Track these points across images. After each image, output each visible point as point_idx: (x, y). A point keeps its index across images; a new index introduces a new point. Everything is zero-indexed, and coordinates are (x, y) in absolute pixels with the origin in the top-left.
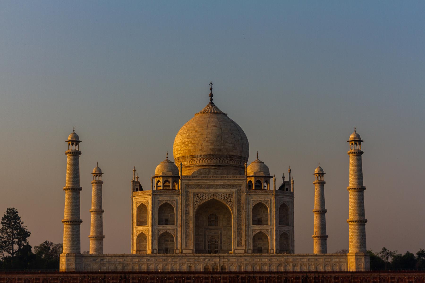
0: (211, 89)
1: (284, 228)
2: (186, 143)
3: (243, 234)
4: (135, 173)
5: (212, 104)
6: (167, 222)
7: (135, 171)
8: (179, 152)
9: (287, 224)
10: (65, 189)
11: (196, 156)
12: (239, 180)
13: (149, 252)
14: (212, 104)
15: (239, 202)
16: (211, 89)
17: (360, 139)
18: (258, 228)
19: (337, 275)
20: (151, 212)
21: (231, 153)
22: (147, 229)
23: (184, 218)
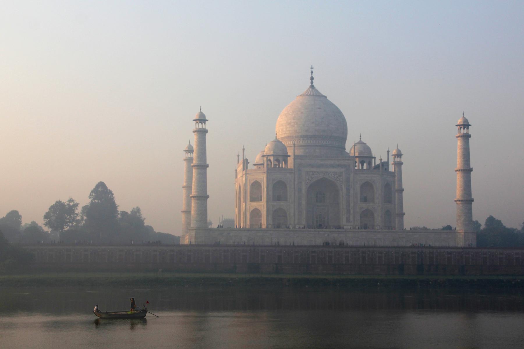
2: (292, 124)
3: (352, 211)
4: (244, 151)
6: (279, 198)
7: (244, 149)
8: (284, 132)
10: (456, 171)
12: (348, 160)
13: (264, 227)
17: (468, 123)
18: (364, 205)
20: (265, 189)
22: (262, 205)
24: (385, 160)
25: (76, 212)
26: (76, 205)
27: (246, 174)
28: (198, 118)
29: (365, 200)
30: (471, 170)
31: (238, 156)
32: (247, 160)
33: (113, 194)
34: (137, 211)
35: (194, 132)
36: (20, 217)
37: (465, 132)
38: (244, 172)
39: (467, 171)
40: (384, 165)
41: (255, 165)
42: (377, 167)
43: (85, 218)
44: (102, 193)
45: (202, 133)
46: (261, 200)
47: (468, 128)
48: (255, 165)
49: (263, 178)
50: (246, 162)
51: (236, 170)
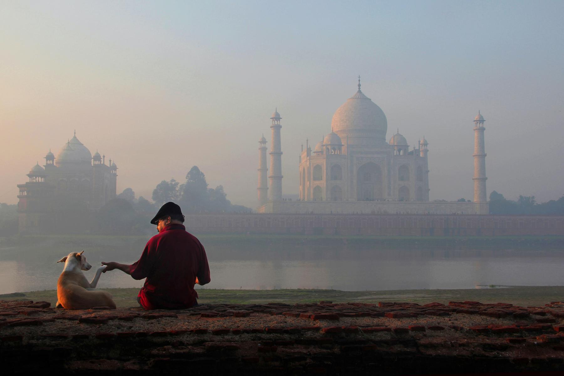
0: (359, 81)
5: (359, 91)
7: (307, 140)
14: (359, 91)
16: (359, 81)
22: (323, 183)
24: (417, 148)
25: (177, 189)
26: (177, 184)
27: (310, 159)
28: (274, 116)
30: (485, 155)
31: (302, 146)
32: (310, 148)
33: (204, 176)
34: (221, 188)
35: (271, 127)
36: (133, 193)
37: (481, 126)
38: (308, 158)
39: (482, 156)
40: (417, 152)
41: (314, 152)
42: (412, 153)
43: (182, 193)
44: (195, 174)
45: (277, 128)
46: (322, 179)
47: (483, 123)
48: (314, 152)
49: (323, 162)
50: (309, 150)
51: (300, 157)
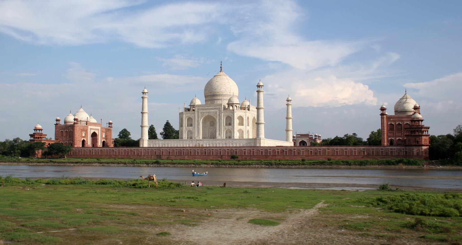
1: (241, 127)
6: (191, 125)
9: (243, 125)
11: (209, 95)
15: (219, 116)
19: (245, 148)
21: (224, 94)
23: (197, 123)
29: (230, 124)
